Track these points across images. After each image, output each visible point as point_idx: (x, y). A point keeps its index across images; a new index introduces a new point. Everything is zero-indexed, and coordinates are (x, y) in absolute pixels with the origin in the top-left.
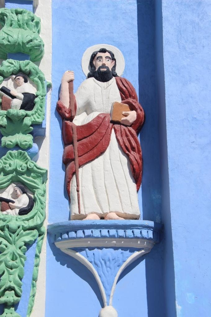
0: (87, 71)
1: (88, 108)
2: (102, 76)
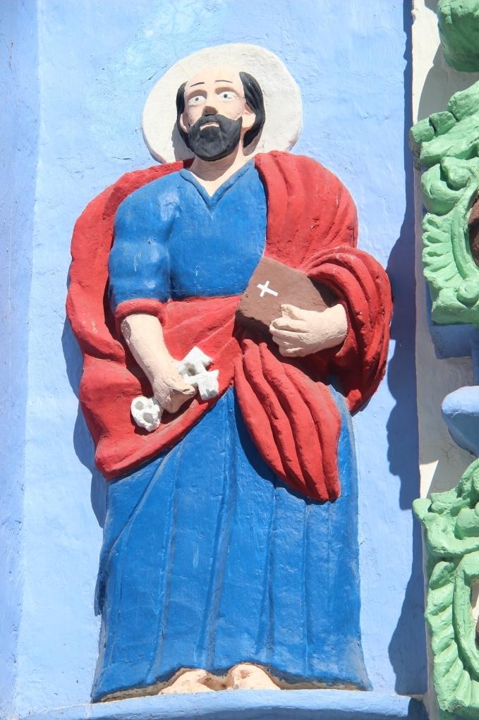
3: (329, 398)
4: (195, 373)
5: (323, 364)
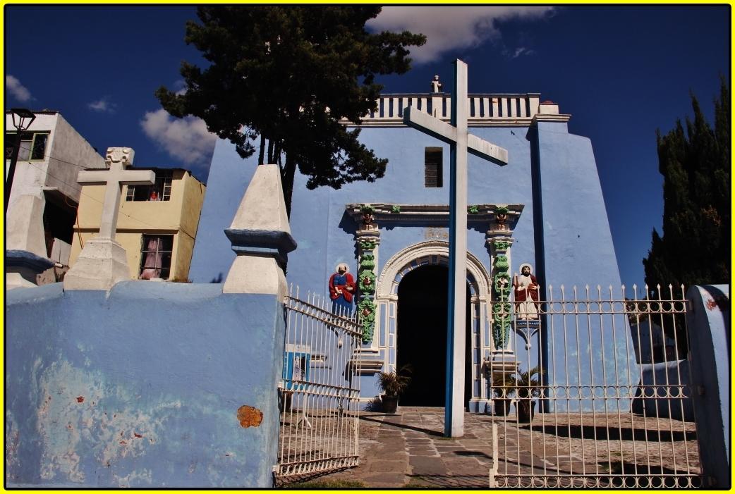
0: (521, 273)
1: (522, 285)
2: (526, 275)
3: (351, 295)
4: (340, 292)
5: (351, 292)
